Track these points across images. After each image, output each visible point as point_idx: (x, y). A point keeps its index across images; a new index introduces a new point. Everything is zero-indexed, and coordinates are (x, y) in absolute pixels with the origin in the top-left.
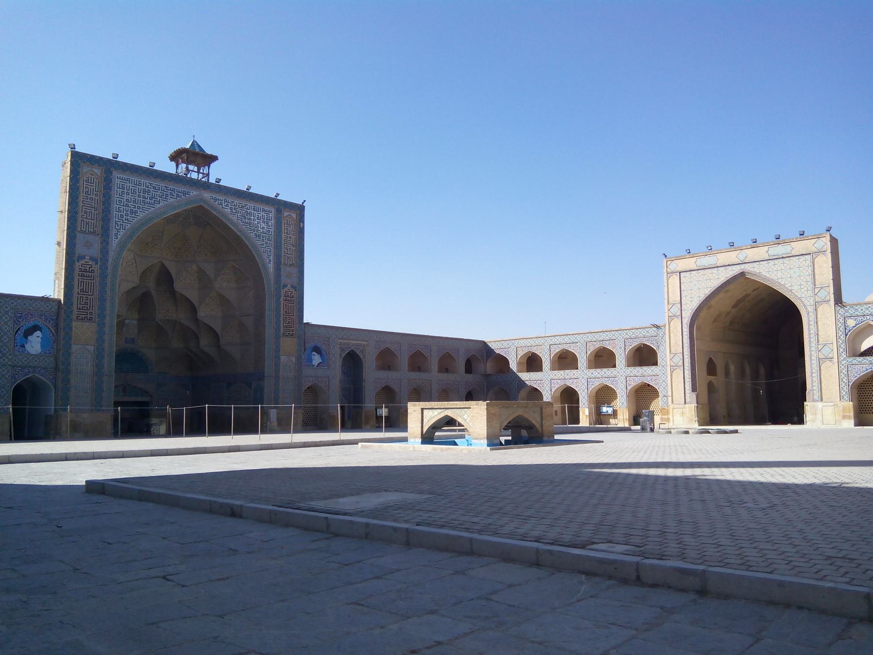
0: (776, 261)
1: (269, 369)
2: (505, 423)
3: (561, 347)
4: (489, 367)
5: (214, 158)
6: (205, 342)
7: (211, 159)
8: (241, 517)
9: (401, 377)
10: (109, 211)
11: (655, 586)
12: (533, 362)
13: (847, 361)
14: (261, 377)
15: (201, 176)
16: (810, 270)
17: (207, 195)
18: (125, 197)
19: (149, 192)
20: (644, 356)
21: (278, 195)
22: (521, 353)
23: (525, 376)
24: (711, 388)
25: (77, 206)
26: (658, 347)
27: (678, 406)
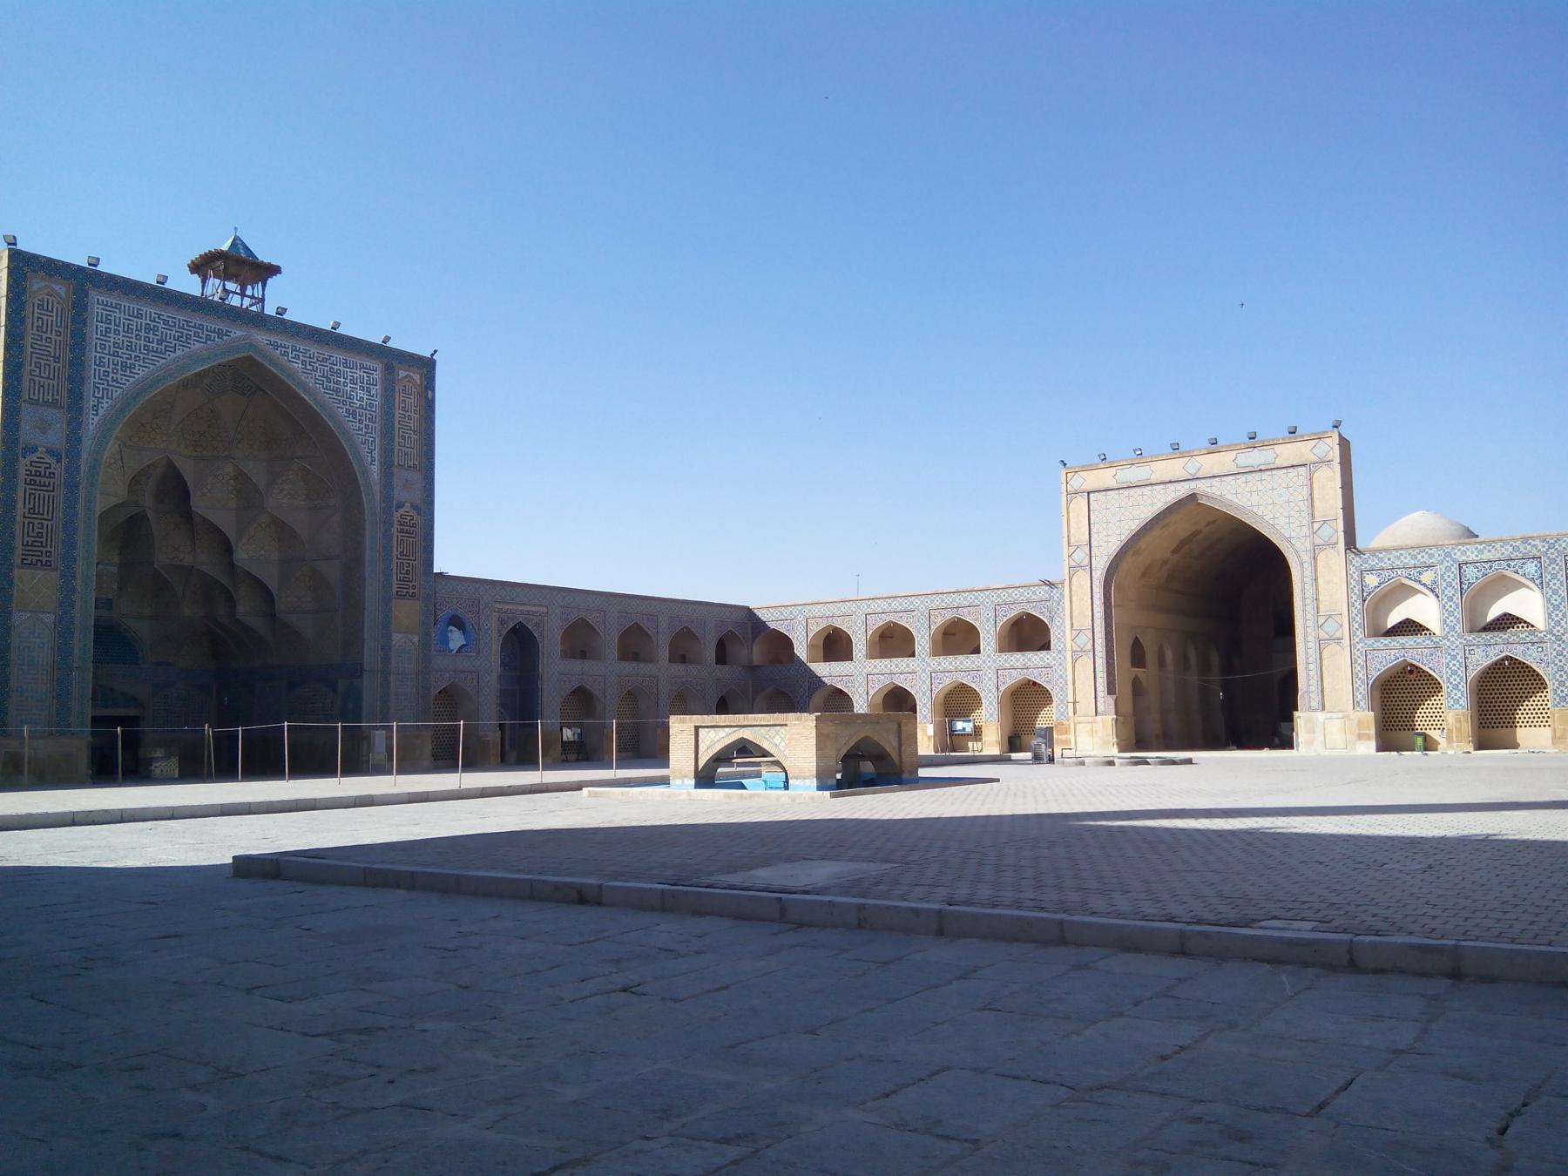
0: (1249, 477)
1: (370, 657)
2: (844, 752)
3: (885, 619)
4: (757, 653)
5: (274, 270)
6: (246, 607)
7: (267, 271)
8: (599, 904)
9: (607, 672)
11: (1379, 971)
14: (357, 671)
15: (247, 302)
16: (1305, 492)
17: (261, 338)
18: (112, 338)
20: (1028, 633)
21: (387, 339)
22: (815, 629)
23: (822, 669)
24: (1137, 688)
25: (22, 352)
26: (1052, 619)
27: (1085, 716)
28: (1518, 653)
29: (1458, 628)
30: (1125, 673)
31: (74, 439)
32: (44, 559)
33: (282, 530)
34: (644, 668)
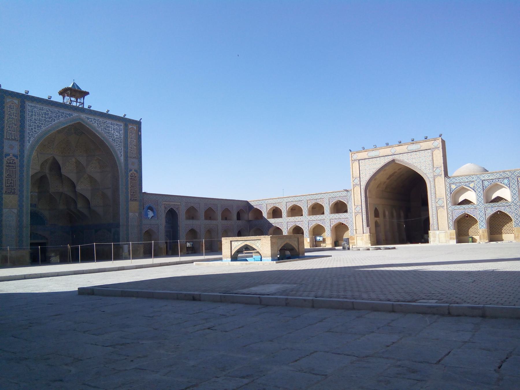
0: (412, 153)
1: (122, 221)
2: (280, 248)
3: (293, 204)
5: (87, 93)
6: (80, 205)
8: (200, 300)
9: (201, 224)
12: (276, 213)
13: (451, 208)
14: (118, 226)
15: (78, 104)
16: (431, 158)
17: (83, 116)
18: (34, 117)
19: (48, 114)
20: (340, 207)
21: (125, 115)
22: (269, 208)
23: (272, 221)
24: (377, 225)
25: (4, 123)
27: (360, 235)
28: (502, 209)
29: (482, 202)
31: (22, 151)
32: (13, 191)
33: (92, 179)
34: (214, 222)
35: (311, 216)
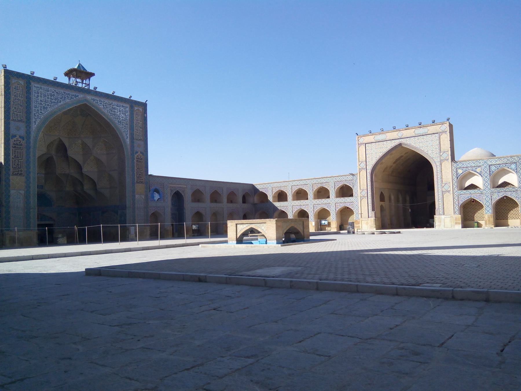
0: (419, 137)
1: (128, 203)
2: (285, 231)
3: (298, 187)
4: (256, 199)
5: (92, 75)
6: (87, 187)
8: (206, 282)
9: (206, 207)
10: (30, 107)
11: (462, 300)
12: (281, 196)
13: (458, 192)
14: (124, 208)
15: (84, 85)
16: (438, 142)
17: (89, 97)
19: (54, 95)
20: (345, 191)
21: (131, 97)
23: (277, 204)
24: (382, 209)
25: (10, 104)
27: (365, 219)
28: (509, 195)
30: (378, 203)
31: (28, 132)
32: (20, 172)
33: (98, 161)
35: (316, 200)
